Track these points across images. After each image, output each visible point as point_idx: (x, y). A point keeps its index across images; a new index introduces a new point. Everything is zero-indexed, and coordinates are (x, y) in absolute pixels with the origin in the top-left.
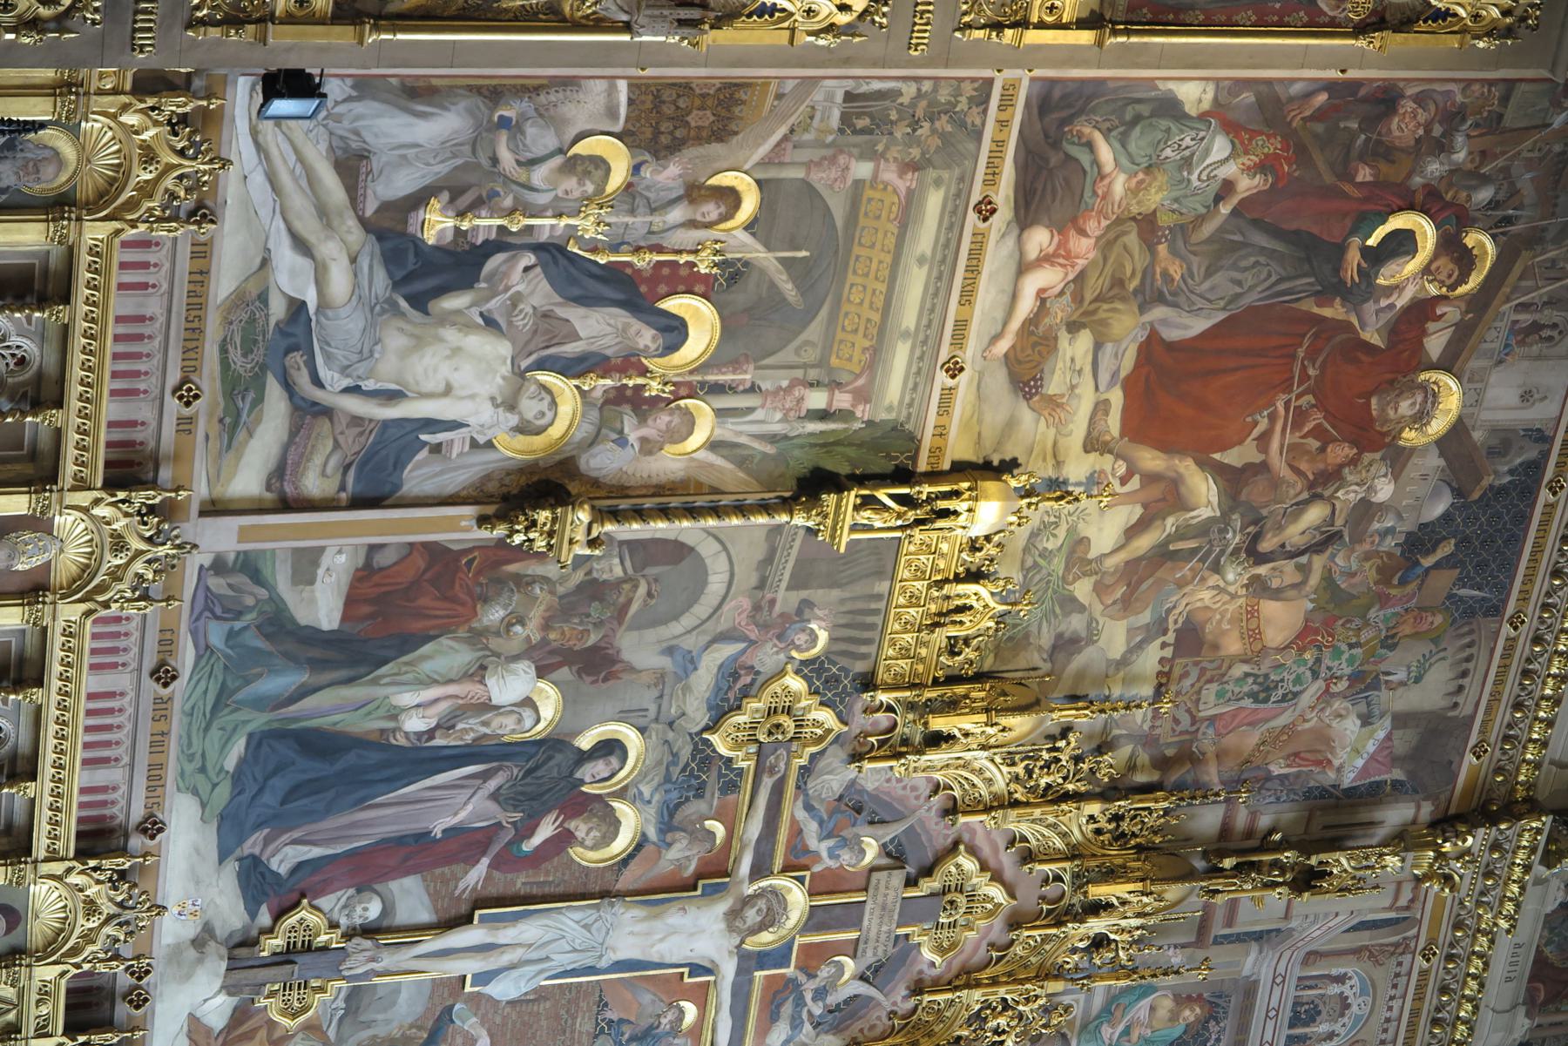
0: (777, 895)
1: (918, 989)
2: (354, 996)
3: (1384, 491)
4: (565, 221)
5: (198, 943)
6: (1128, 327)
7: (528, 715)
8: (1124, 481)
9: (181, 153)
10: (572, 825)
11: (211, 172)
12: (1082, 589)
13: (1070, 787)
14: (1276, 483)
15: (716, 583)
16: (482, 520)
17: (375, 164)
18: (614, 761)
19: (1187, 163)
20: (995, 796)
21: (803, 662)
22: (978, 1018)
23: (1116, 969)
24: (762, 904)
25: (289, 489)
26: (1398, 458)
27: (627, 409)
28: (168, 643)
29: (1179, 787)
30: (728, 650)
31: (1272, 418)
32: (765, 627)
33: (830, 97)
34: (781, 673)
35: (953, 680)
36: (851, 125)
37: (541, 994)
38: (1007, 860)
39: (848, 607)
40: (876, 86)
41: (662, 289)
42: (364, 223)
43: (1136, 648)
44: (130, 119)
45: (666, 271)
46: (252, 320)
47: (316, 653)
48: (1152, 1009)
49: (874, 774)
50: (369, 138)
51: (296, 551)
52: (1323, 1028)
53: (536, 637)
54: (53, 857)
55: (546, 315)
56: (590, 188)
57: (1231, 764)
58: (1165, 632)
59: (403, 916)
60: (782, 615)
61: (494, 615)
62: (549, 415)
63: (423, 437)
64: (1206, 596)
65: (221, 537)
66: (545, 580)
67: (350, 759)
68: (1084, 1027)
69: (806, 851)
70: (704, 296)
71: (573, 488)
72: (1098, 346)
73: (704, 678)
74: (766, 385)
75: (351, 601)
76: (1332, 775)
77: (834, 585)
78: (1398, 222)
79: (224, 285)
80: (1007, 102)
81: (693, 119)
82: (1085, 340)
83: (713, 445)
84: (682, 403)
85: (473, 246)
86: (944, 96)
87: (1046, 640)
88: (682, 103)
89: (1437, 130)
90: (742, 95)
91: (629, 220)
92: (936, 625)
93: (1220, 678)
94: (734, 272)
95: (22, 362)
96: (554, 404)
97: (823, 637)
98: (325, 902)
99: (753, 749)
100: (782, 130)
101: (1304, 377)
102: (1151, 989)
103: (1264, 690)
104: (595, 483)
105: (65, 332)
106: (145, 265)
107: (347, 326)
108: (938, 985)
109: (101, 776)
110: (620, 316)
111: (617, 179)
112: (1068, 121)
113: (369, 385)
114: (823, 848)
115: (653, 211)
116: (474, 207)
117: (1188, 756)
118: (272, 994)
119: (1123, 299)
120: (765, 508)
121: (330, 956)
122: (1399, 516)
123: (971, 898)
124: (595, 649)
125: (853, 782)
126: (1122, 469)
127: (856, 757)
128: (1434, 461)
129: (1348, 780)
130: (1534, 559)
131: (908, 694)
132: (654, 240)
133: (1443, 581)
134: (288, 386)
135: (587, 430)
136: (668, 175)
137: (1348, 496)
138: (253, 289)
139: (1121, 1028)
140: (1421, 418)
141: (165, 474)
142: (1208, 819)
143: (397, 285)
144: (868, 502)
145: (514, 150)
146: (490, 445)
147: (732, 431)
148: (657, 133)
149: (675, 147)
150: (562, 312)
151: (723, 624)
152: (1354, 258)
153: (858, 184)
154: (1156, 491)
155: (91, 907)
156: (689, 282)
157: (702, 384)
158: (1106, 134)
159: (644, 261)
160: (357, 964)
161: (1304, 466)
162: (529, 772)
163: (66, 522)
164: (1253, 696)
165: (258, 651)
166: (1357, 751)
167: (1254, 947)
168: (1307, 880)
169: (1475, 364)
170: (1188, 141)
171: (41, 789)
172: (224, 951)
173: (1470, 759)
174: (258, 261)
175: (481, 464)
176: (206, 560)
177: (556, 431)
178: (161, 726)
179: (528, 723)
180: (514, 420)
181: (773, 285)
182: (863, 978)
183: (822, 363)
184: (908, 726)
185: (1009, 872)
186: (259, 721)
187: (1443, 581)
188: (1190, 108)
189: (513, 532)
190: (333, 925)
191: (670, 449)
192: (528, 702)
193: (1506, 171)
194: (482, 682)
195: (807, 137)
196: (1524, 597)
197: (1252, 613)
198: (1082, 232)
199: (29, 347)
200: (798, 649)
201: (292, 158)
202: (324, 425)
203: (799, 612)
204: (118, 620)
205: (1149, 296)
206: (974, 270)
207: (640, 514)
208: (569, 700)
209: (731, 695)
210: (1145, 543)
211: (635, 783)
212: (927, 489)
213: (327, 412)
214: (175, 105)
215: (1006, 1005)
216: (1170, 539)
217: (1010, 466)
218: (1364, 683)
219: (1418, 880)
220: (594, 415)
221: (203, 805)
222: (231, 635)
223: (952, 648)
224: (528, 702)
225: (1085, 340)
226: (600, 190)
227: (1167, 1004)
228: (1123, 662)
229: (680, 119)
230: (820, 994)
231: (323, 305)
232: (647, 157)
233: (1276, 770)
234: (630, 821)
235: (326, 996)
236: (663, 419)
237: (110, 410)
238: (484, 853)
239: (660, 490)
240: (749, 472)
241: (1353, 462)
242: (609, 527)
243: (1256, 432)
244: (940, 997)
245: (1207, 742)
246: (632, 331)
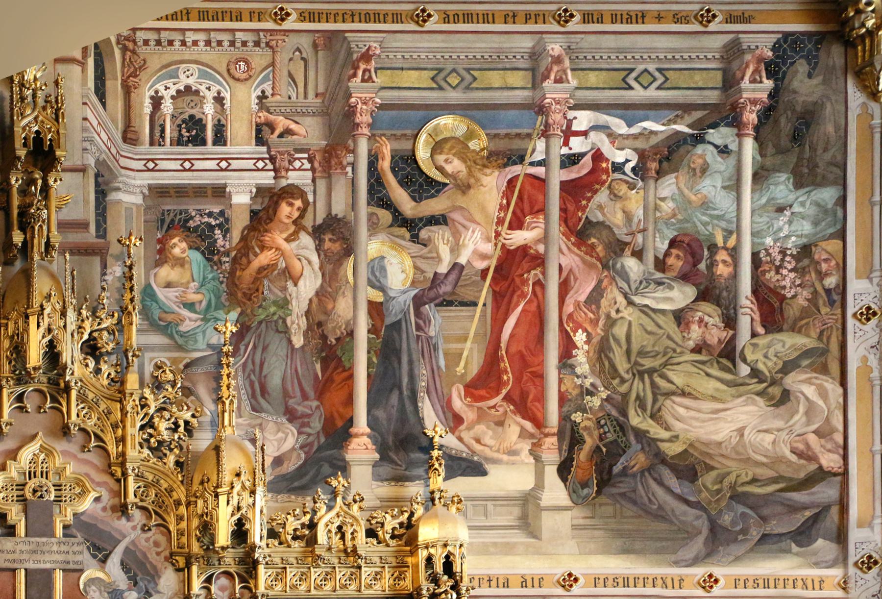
1: (123, 509)
22: (158, 449)
48: (169, 285)
123: (32, 475)
139: (185, 313)
167: (113, 196)
182: (104, 561)
227: (166, 272)
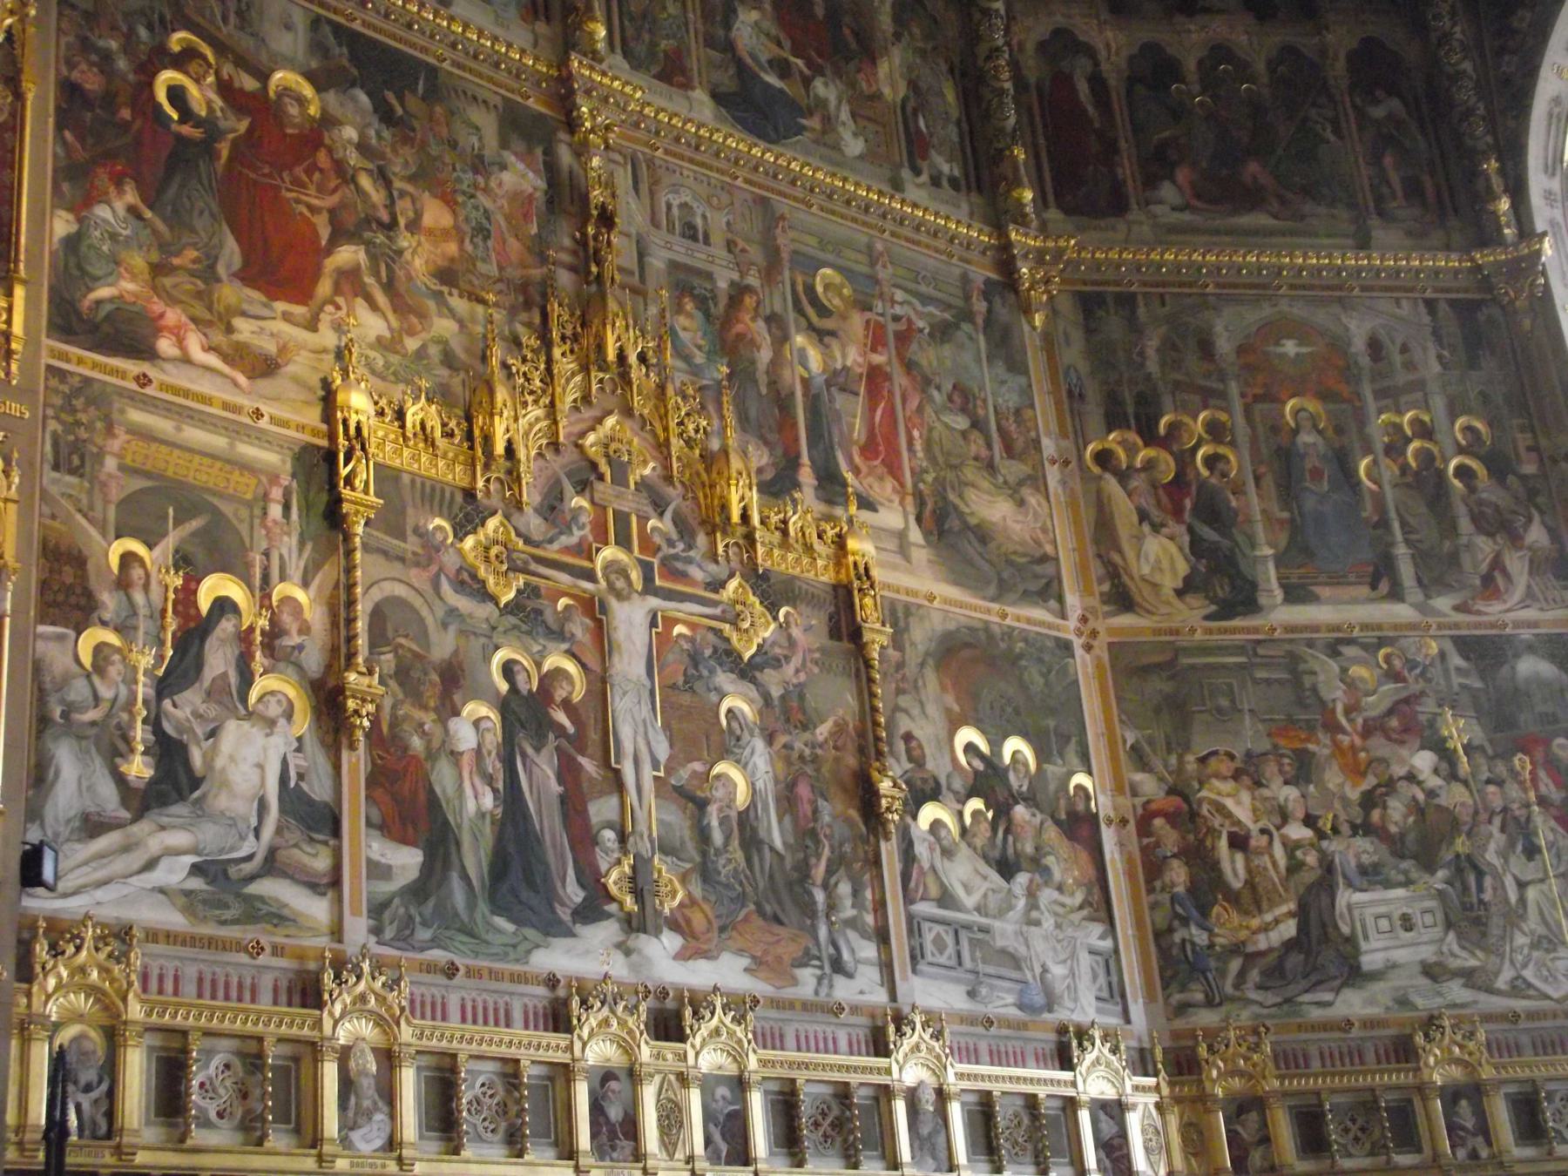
0: (609, 566)
1: (669, 479)
2: (666, 849)
3: (350, 133)
4: (141, 678)
5: (628, 953)
6: (230, 292)
7: (484, 725)
8: (338, 308)
9: (78, 949)
10: (558, 699)
11: (94, 927)
12: (412, 344)
13: (542, 366)
14: (343, 205)
15: (400, 590)
16: (352, 747)
17: (92, 809)
18: (516, 668)
19: (113, 237)
20: (547, 416)
21: (455, 536)
22: (689, 443)
23: (659, 350)
24: (613, 577)
25: (325, 881)
26: (328, 121)
27: (277, 642)
28: (430, 968)
29: (544, 296)
30: (446, 588)
31: (298, 201)
32: (430, 561)
33: (54, 482)
34: (460, 552)
35: (469, 436)
36: (78, 468)
37: (666, 726)
38: (588, 413)
39: (418, 501)
40: (48, 448)
41: (192, 612)
42: (136, 819)
43: (452, 314)
44: (52, 982)
45: (180, 608)
46: (205, 902)
47: (438, 865)
48: (685, 329)
49: (531, 496)
50: (72, 813)
51: (368, 877)
52: (699, 222)
53: (433, 716)
54: (570, 1048)
55: (209, 693)
56: (116, 657)
57: (529, 259)
58: (441, 293)
59: (613, 815)
60: (423, 547)
61: (417, 743)
62: (280, 697)
63: (292, 784)
64: (418, 263)
65: (357, 929)
66: (394, 707)
67: (511, 848)
68: (694, 374)
69: (580, 544)
70: (199, 582)
71: (331, 683)
72: (244, 314)
73: (463, 603)
74: (264, 545)
75: (404, 841)
76: (538, 194)
77: (403, 512)
78: (162, 96)
79: (174, 919)
80: (65, 357)
81: (69, 580)
82: (238, 322)
83: (305, 584)
84: (275, 604)
85: (156, 742)
86: (58, 401)
87: (445, 372)
88: (56, 588)
89: (94, 58)
90: (51, 544)
91: (141, 633)
92: (433, 445)
93: (472, 260)
94: (182, 560)
95: (227, 1066)
96: (272, 693)
97: (438, 521)
98: (603, 867)
99: (511, 575)
100: (79, 517)
101: (269, 176)
102: (672, 329)
103: (482, 232)
104: (329, 667)
105: (208, 1033)
106: (161, 978)
107: (210, 836)
108: (667, 467)
109: (517, 1015)
110: (211, 643)
111: (112, 638)
112: (78, 314)
113: (254, 822)
114: (577, 534)
115: (135, 614)
116: (127, 740)
117: (524, 287)
118: (662, 903)
119: (210, 294)
120: (349, 553)
121: (639, 865)
122: (369, 125)
123: (612, 439)
124: (441, 676)
125: (536, 510)
126: (329, 308)
127: (519, 506)
128: (331, 97)
129: (542, 184)
130: (400, 40)
131: (478, 468)
132: (157, 615)
133: (413, 103)
134: (252, 878)
135: (291, 670)
136: (109, 601)
137: (353, 158)
138: (182, 900)
139: (696, 351)
140: (301, 101)
141: (312, 966)
142: (565, 278)
143: (182, 798)
144: (349, 481)
145: (86, 709)
146: (299, 739)
147: (296, 572)
148: (78, 607)
149: (89, 595)
150: (207, 683)
151: (427, 588)
152: (186, 130)
153: (122, 468)
154: (346, 287)
155: (606, 1023)
156: (187, 594)
157: (262, 589)
158: (90, 290)
159: (172, 623)
160: (645, 848)
161: (332, 184)
162: (523, 727)
163: (343, 1035)
164: (486, 238)
165: (436, 906)
166: (523, 176)
167: (648, 259)
168: (607, 219)
169: (264, 57)
170: (97, 233)
171: (526, 1057)
172: (633, 936)
173: (531, 102)
174: (161, 896)
175: (311, 745)
176: (373, 939)
177: (291, 692)
178: (485, 973)
179: (489, 724)
180: (282, 722)
181: (194, 534)
182: (661, 514)
183: (249, 505)
184: (499, 469)
185: (595, 412)
186: (483, 907)
187: (413, 103)
188: (74, 228)
189: (361, 726)
190: (619, 862)
191: (307, 615)
192: (476, 723)
193: (126, 15)
194: (461, 754)
195: (85, 501)
196: (424, 50)
197: (430, 232)
198: (162, 316)
199: (217, 1061)
200: (446, 538)
201: (85, 869)
202: (282, 855)
203: (421, 536)
204: (412, 1002)
205: (208, 274)
206: (186, 394)
207: (351, 639)
208: (476, 695)
209: (476, 586)
210: (381, 299)
211: (531, 655)
212: (341, 440)
213: (272, 853)
214: (41, 950)
215: (681, 423)
216: (379, 280)
217: (326, 384)
218: (479, 165)
219: (607, 147)
220: (282, 665)
221: (537, 946)
222: (425, 924)
223: (449, 435)
224: (476, 723)
225: (238, 322)
226: (118, 650)
227: (682, 321)
228: (462, 324)
229: (69, 590)
230: (671, 544)
231: (195, 851)
232: (95, 615)
233: (534, 230)
234: (556, 660)
235: (664, 868)
236: (287, 619)
237: (265, 1003)
238: (574, 759)
239: (334, 624)
240: (323, 564)
241: (330, 151)
242: (360, 660)
243: (308, 214)
244: (675, 466)
245: (514, 273)
246: (222, 635)
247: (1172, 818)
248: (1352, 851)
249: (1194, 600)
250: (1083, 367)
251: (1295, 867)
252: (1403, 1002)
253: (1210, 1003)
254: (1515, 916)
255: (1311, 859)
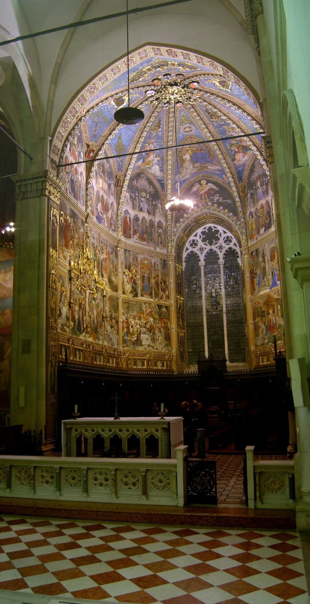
247: (126, 322)
248: (144, 330)
249: (131, 294)
250: (124, 259)
251: (137, 331)
252: (146, 349)
253: (127, 346)
254: (158, 340)
255: (139, 330)
